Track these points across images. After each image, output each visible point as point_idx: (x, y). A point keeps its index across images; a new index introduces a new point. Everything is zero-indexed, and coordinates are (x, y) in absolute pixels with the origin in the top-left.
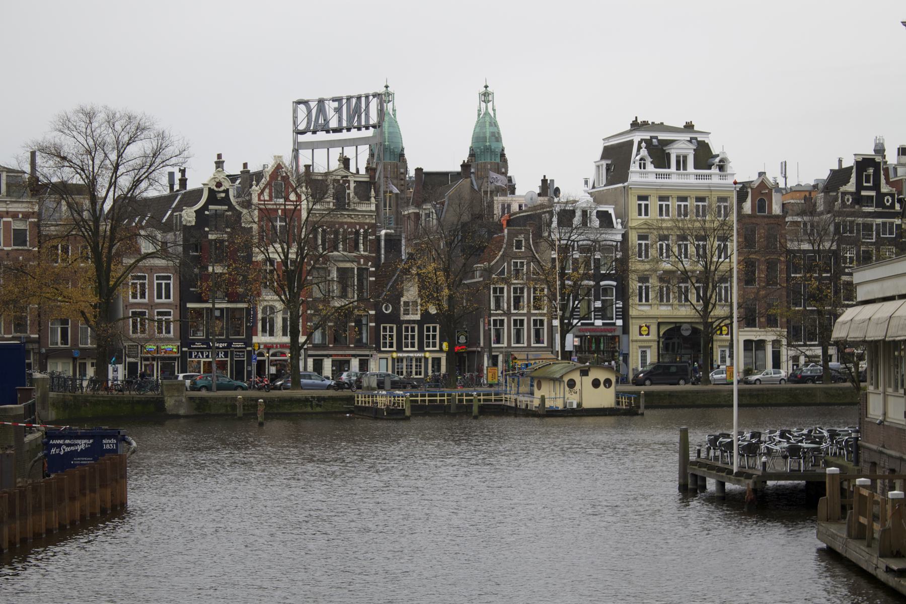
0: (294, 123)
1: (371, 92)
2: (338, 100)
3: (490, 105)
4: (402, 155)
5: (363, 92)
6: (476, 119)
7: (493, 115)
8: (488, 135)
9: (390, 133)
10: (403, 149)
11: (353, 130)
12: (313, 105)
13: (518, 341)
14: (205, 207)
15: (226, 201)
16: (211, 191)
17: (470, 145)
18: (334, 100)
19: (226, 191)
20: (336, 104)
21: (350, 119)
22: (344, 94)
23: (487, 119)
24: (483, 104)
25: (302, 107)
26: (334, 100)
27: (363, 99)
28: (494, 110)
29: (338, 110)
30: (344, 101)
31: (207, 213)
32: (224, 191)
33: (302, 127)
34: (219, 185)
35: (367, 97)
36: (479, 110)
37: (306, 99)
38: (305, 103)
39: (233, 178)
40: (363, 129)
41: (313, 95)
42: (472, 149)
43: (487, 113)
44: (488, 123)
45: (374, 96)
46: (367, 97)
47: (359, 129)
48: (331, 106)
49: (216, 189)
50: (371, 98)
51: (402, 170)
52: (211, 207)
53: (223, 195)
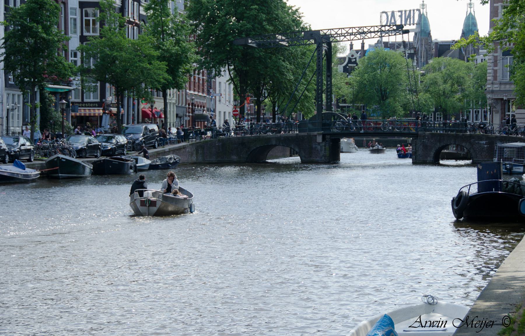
0: (381, 22)
1: (415, 9)
2: (401, 12)
3: (472, 9)
4: (429, 34)
5: (412, 9)
6: (465, 16)
7: (473, 14)
8: (471, 24)
9: (424, 23)
10: (430, 31)
11: (407, 25)
12: (390, 14)
13: (477, 120)
14: (347, 65)
15: (355, 62)
16: (349, 58)
17: (462, 28)
18: (399, 11)
19: (356, 58)
20: (400, 14)
21: (406, 20)
22: (403, 9)
23: (470, 16)
24: (469, 9)
25: (384, 15)
26: (399, 11)
27: (412, 12)
28: (474, 12)
29: (401, 16)
30: (403, 12)
31: (347, 67)
32: (354, 59)
33: (384, 24)
34: (353, 56)
35: (414, 10)
36: (467, 12)
37: (386, 11)
38: (386, 13)
39: (357, 52)
40: (412, 25)
41: (389, 10)
42: (463, 31)
43: (470, 13)
44: (471, 18)
45: (417, 10)
46: (414, 10)
47: (410, 25)
48: (397, 15)
49: (351, 58)
50: (415, 11)
51: (430, 41)
52: (349, 65)
53: (354, 60)
